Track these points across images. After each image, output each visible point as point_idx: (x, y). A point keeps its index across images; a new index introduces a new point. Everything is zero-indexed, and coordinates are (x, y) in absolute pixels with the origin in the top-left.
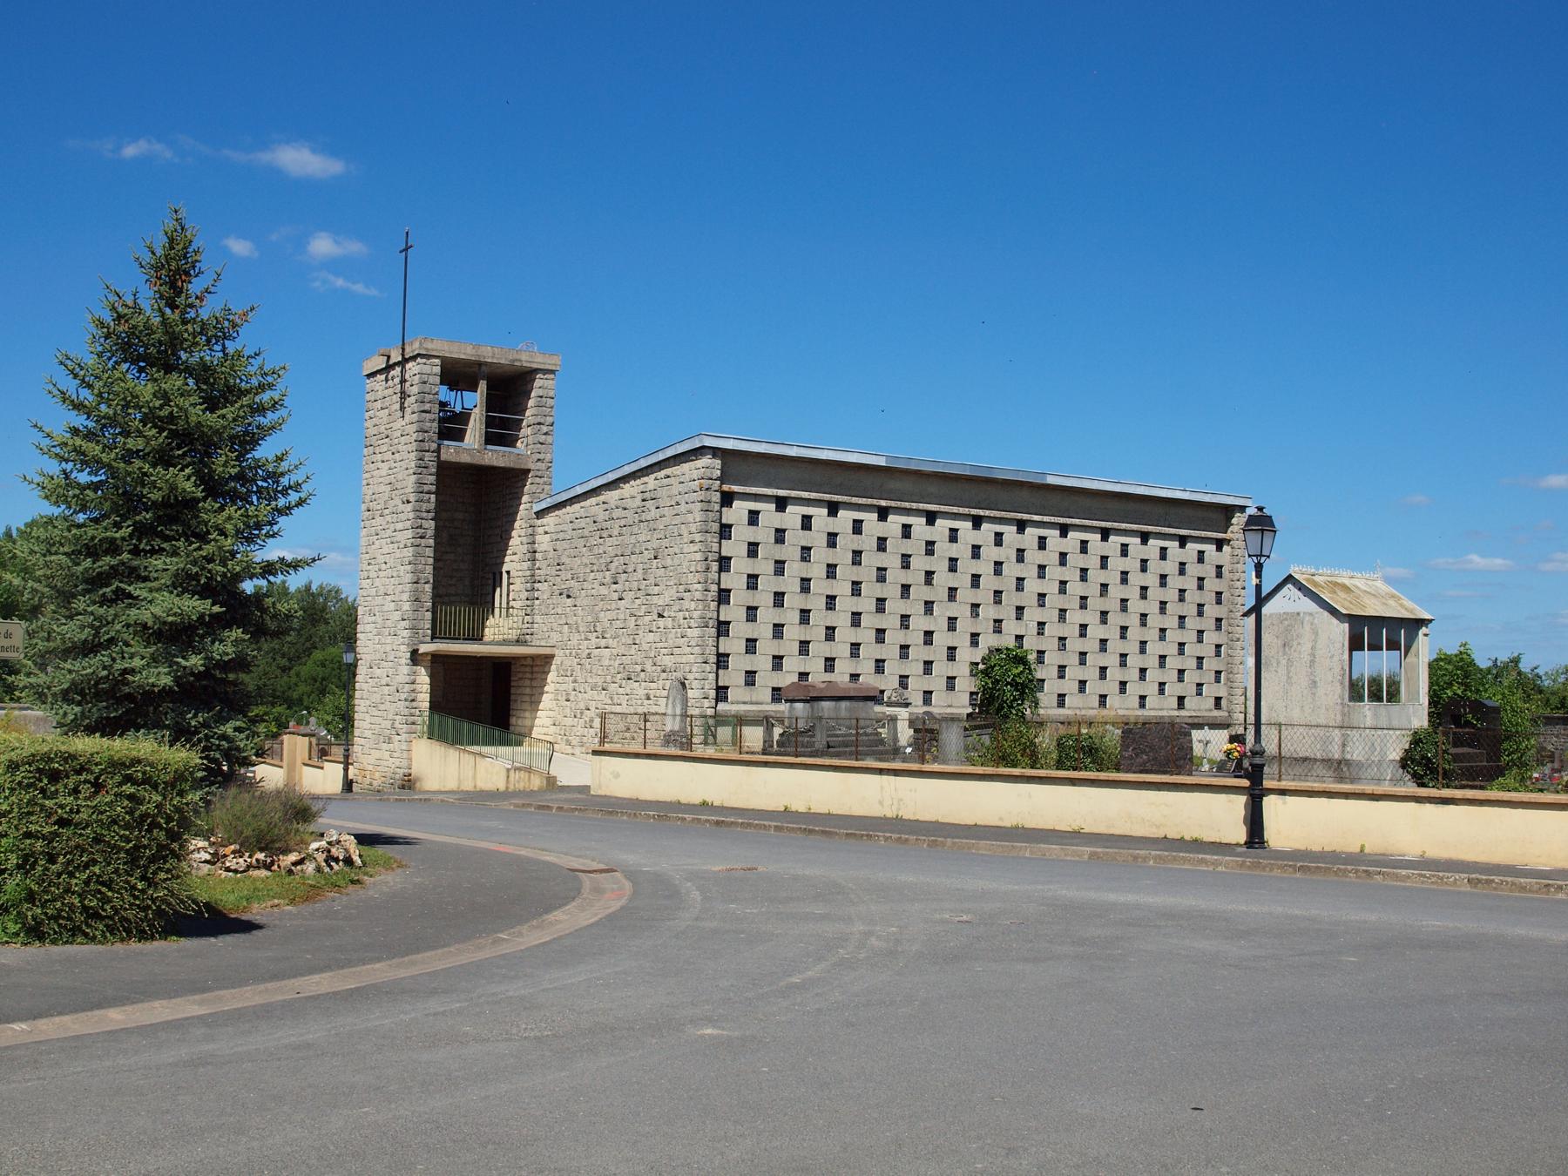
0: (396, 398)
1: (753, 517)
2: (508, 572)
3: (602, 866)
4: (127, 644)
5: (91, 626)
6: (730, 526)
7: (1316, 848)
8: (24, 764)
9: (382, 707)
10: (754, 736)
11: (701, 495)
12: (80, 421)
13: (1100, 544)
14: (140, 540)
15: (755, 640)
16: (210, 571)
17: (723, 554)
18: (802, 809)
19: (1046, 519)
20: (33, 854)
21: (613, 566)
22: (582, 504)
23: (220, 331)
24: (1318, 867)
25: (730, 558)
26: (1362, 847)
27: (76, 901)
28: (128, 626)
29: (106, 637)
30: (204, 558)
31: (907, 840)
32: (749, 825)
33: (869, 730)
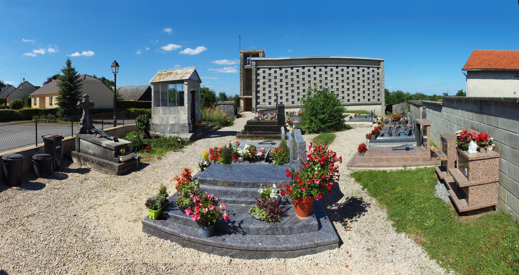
1: (264, 72)
13: (346, 69)
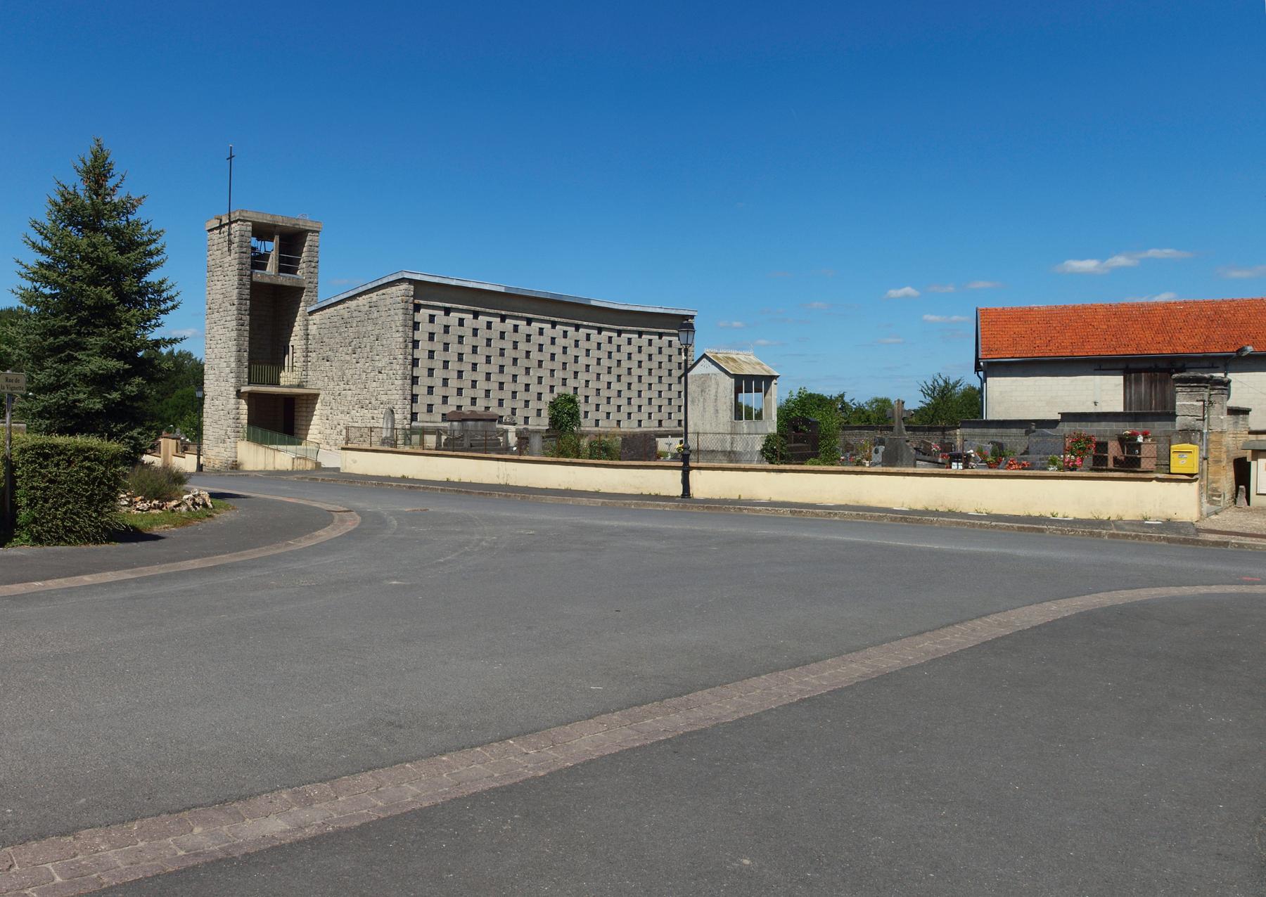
0: (226, 244)
2: (293, 346)
3: (346, 509)
4: (75, 385)
5: (55, 375)
6: (419, 323)
7: (717, 497)
8: (29, 450)
9: (219, 423)
10: (431, 440)
11: (402, 305)
12: (44, 259)
14: (81, 327)
15: (433, 387)
16: (122, 345)
17: (415, 339)
18: (456, 480)
19: (590, 324)
20: (35, 498)
21: (353, 344)
22: (335, 308)
23: (126, 208)
24: (715, 507)
25: (419, 341)
26: (740, 496)
27: (60, 523)
28: (76, 375)
29: (63, 382)
30: (119, 338)
31: (510, 496)
32: (427, 488)
33: (493, 437)
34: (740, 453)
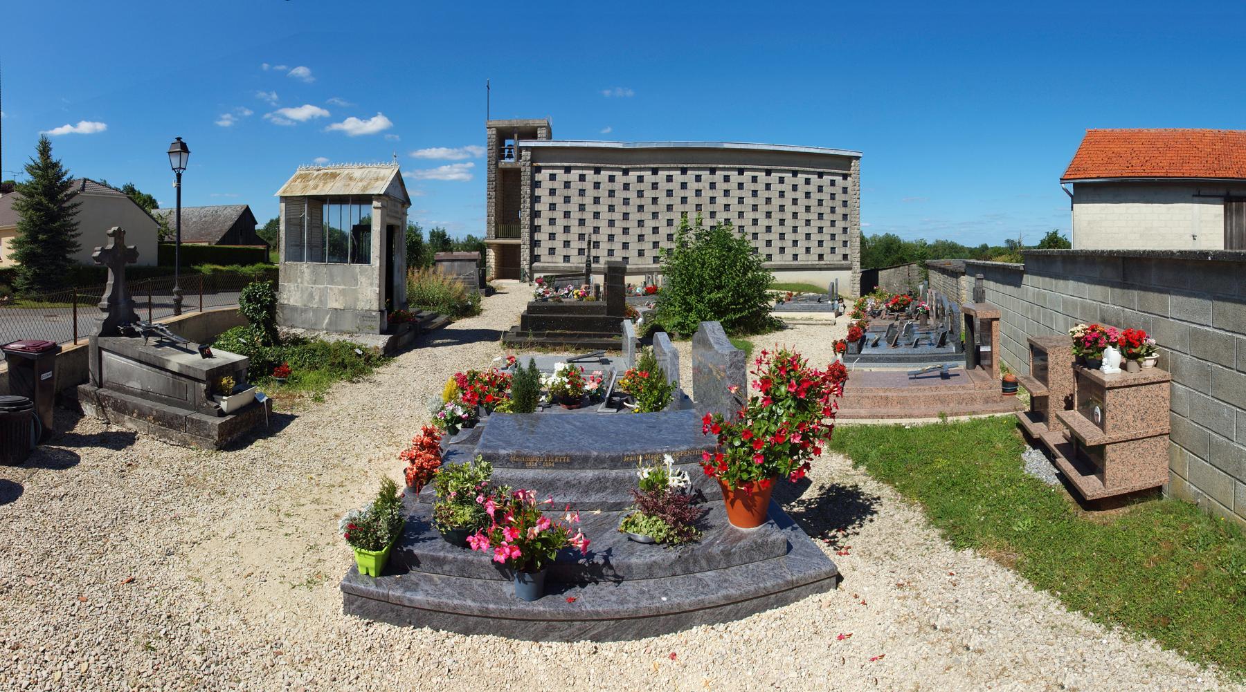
13: (765, 177)
34: (294, 309)
